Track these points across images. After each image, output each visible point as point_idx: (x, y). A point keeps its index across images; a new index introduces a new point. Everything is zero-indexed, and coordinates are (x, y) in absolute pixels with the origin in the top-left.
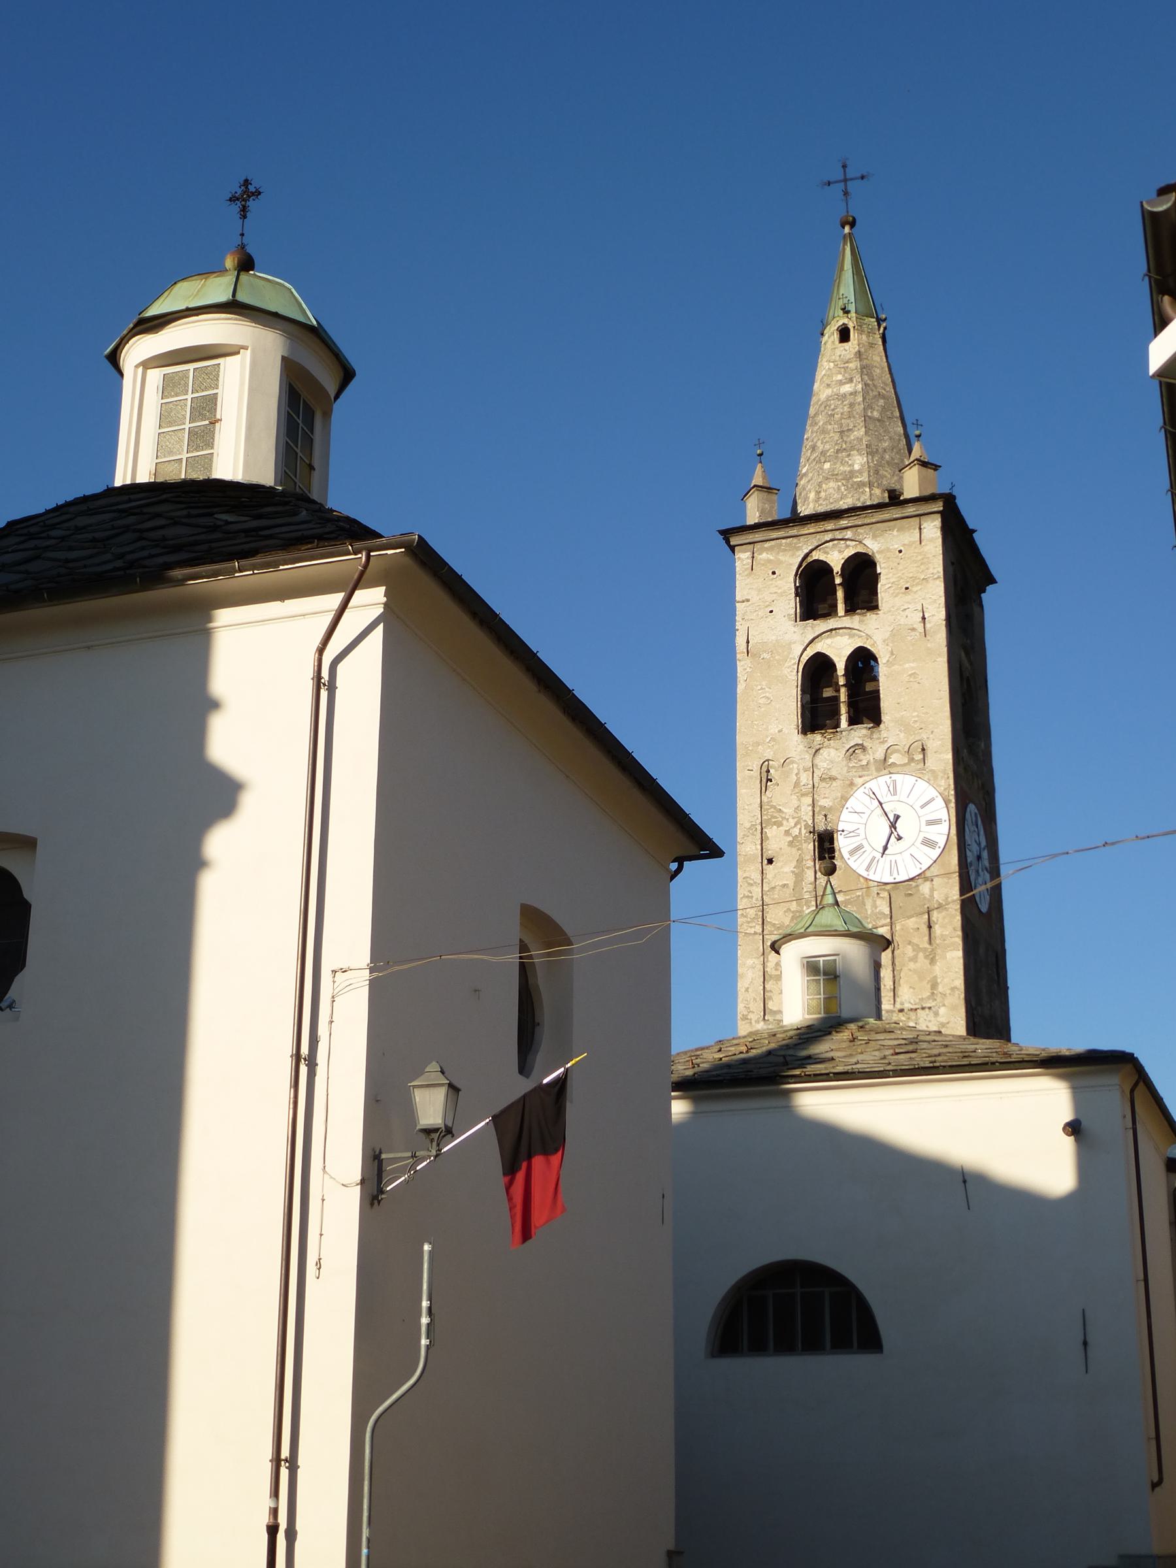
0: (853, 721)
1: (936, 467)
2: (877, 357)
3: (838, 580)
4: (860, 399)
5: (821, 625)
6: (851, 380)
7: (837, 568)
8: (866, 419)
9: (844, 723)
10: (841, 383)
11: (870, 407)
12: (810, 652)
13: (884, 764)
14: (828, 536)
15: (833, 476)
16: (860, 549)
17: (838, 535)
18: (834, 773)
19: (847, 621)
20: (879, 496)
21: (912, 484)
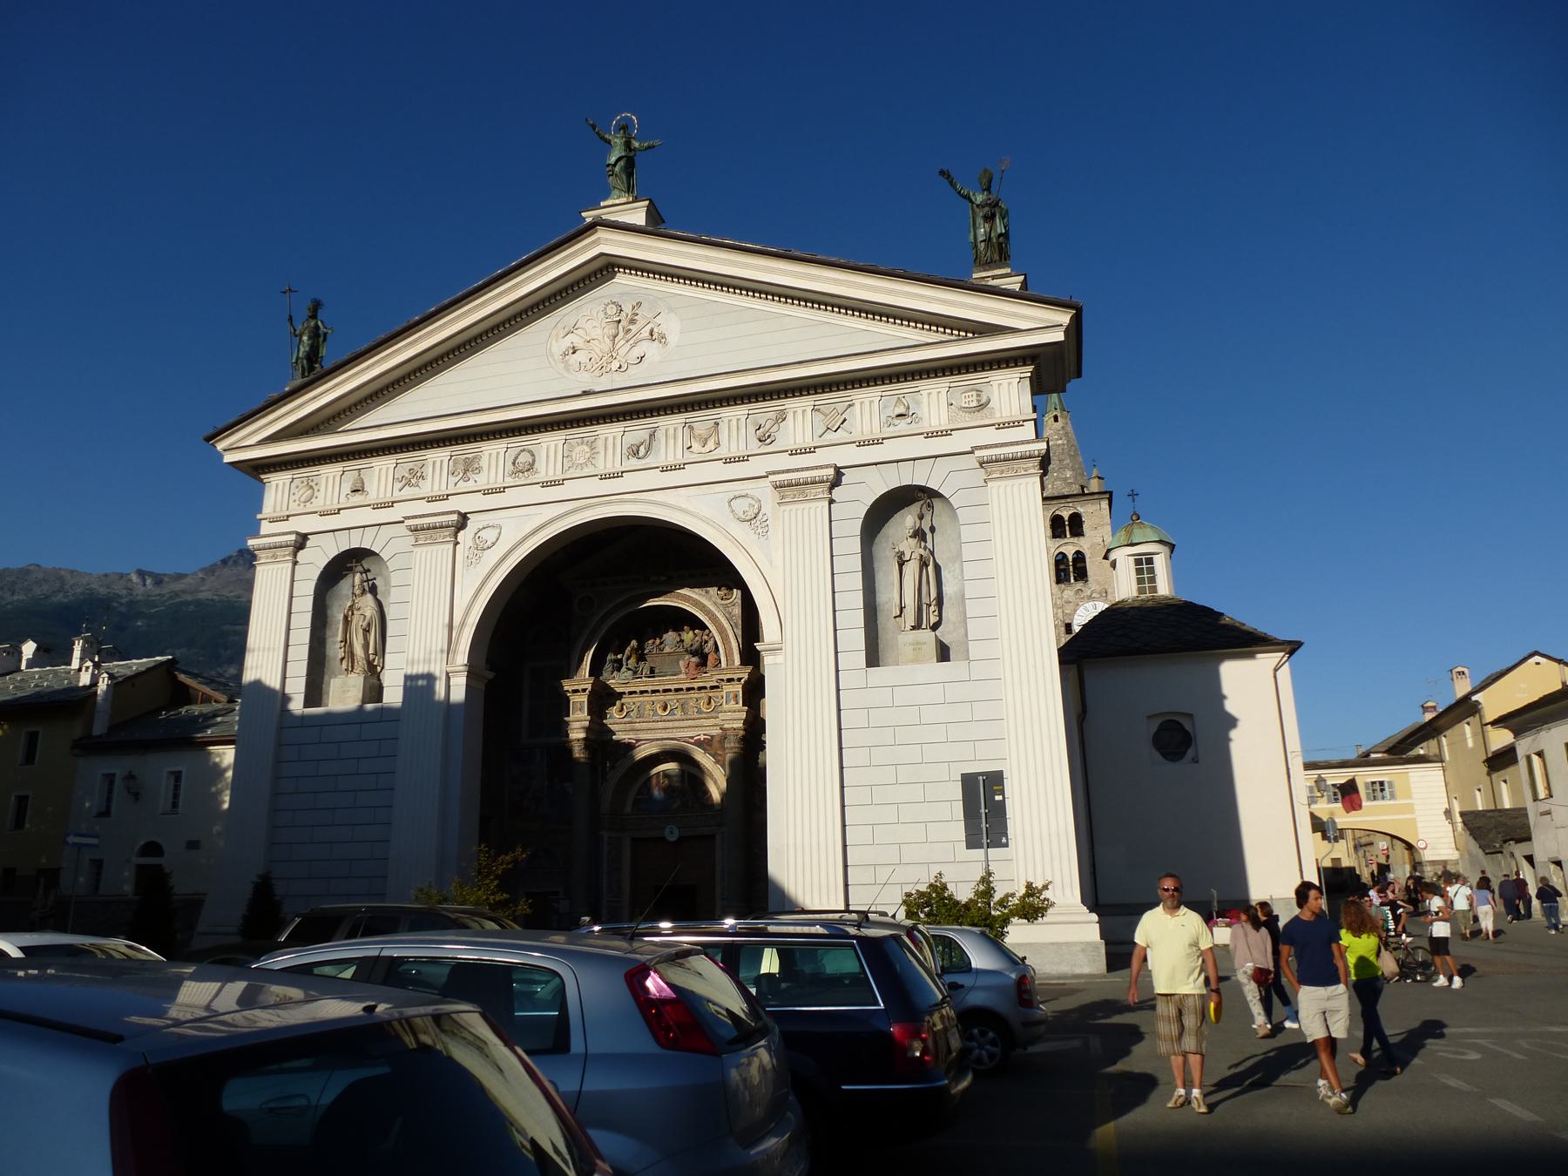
0: (1076, 580)
1: (1102, 479)
2: (1070, 428)
3: (1067, 523)
4: (1066, 447)
5: (1062, 541)
6: (1061, 439)
7: (1066, 518)
8: (1070, 456)
9: (1072, 581)
10: (1057, 440)
11: (1069, 451)
12: (1057, 552)
13: (1090, 598)
14: (1062, 505)
15: (1057, 479)
16: (1075, 511)
17: (1066, 505)
18: (1070, 600)
19: (1072, 540)
20: (1076, 489)
21: (1094, 486)
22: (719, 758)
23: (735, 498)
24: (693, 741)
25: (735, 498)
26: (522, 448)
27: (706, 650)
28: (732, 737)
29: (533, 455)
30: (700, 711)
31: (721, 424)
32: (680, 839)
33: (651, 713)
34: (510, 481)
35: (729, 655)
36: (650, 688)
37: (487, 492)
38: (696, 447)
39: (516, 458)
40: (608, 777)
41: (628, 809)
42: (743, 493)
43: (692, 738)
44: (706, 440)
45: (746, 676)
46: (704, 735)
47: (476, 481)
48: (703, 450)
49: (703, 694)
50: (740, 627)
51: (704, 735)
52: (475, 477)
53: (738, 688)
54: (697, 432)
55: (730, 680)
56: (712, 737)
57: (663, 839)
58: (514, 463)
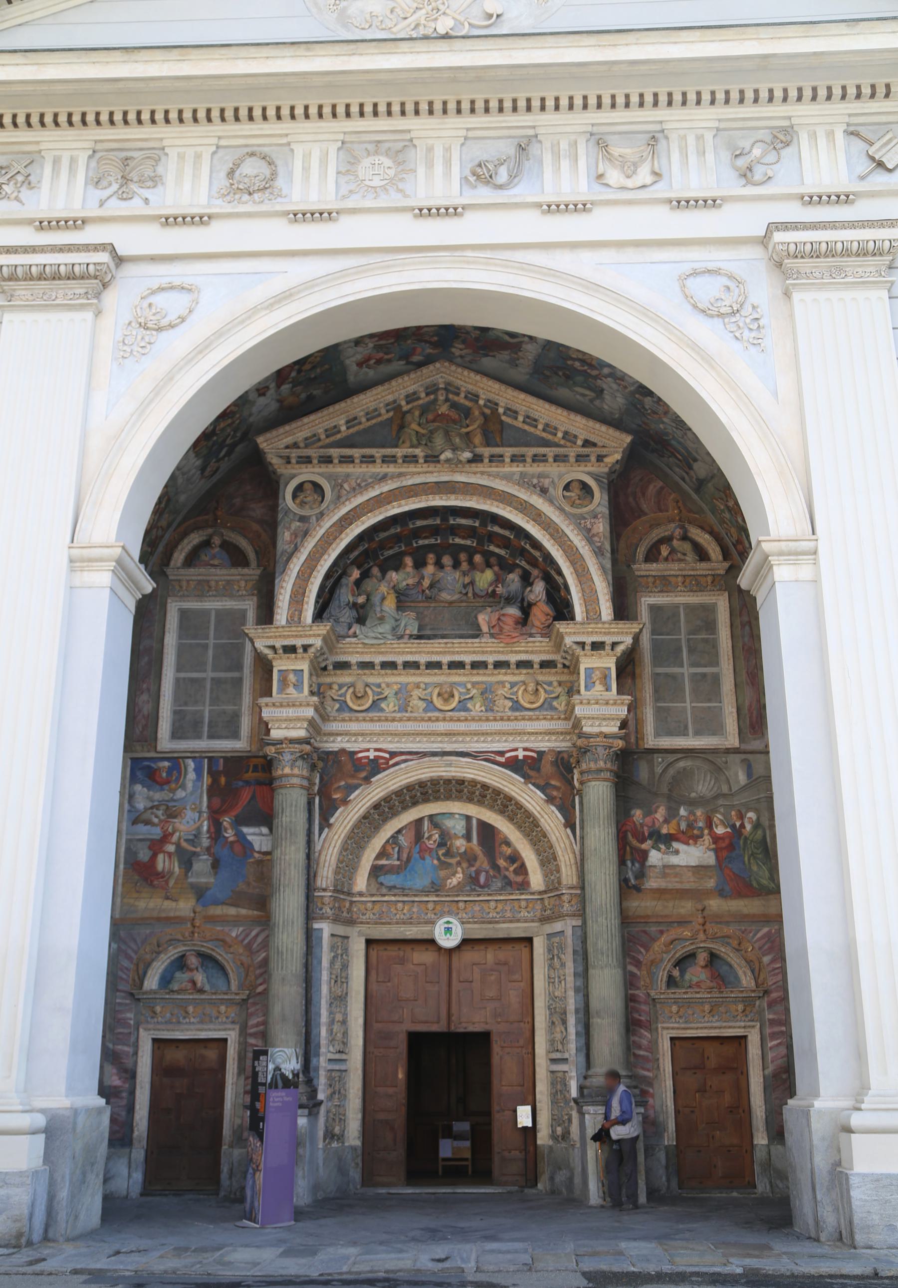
22: (555, 793)
23: (695, 273)
24: (502, 760)
25: (695, 273)
26: (249, 150)
27: (532, 597)
28: (600, 751)
29: (270, 163)
30: (517, 706)
31: (663, 143)
32: (465, 942)
33: (422, 705)
34: (220, 206)
35: (591, 600)
36: (423, 659)
37: (170, 221)
38: (614, 176)
39: (237, 165)
40: (332, 821)
41: (361, 882)
42: (710, 266)
43: (501, 753)
44: (635, 165)
45: (629, 640)
46: (525, 749)
47: (146, 201)
48: (630, 183)
49: (521, 676)
50: (609, 555)
51: (525, 749)
52: (146, 193)
53: (610, 663)
54: (616, 151)
55: (597, 646)
56: (541, 754)
57: (432, 942)
58: (231, 173)
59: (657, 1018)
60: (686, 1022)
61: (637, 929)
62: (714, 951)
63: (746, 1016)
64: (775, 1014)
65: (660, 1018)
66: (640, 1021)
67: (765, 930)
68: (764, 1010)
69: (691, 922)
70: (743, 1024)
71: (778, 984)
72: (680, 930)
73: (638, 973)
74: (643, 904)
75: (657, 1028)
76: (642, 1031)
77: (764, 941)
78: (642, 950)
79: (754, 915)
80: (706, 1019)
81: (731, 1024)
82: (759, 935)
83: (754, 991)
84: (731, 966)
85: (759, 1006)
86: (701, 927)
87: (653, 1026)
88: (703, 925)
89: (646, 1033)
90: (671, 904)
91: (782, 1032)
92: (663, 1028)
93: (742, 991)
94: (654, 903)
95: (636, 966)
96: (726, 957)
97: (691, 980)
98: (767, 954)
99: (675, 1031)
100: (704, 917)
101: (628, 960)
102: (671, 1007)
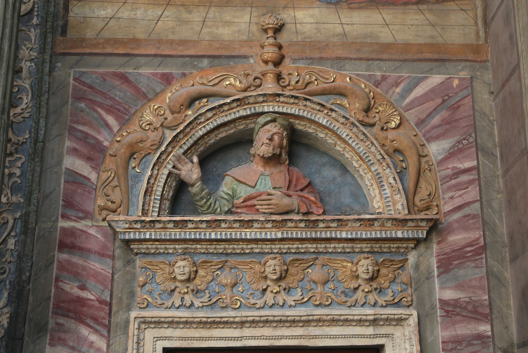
59: (132, 294)
60: (212, 306)
61: (101, 70)
62: (300, 126)
63: (380, 291)
64: (460, 287)
65: (141, 295)
66: (81, 301)
67: (436, 80)
68: (429, 277)
69: (246, 57)
70: (369, 311)
71: (467, 211)
72: (213, 76)
73: (93, 176)
74: (125, 13)
75: (127, 322)
76: (84, 331)
77: (430, 105)
78: (111, 120)
79: (407, 47)
80: (269, 297)
81: (336, 311)
82: (419, 91)
83: (403, 222)
84: (344, 169)
85: (417, 267)
86: (271, 66)
87: (118, 318)
88: (277, 63)
89: (93, 337)
90: (197, 16)
91: (480, 337)
92: (146, 323)
93: (371, 221)
94: (154, 12)
95: (89, 159)
96: (331, 140)
97: (233, 197)
98: (437, 138)
99: (178, 332)
100: (280, 47)
101: (68, 143)
102: (172, 265)
